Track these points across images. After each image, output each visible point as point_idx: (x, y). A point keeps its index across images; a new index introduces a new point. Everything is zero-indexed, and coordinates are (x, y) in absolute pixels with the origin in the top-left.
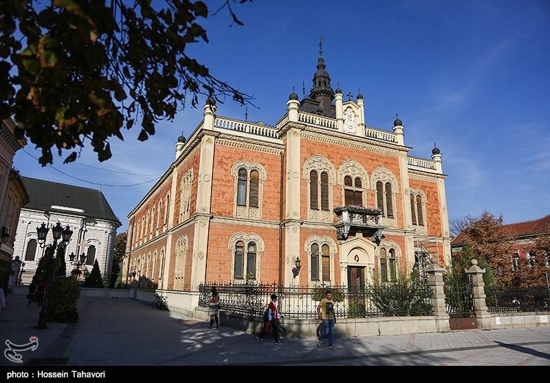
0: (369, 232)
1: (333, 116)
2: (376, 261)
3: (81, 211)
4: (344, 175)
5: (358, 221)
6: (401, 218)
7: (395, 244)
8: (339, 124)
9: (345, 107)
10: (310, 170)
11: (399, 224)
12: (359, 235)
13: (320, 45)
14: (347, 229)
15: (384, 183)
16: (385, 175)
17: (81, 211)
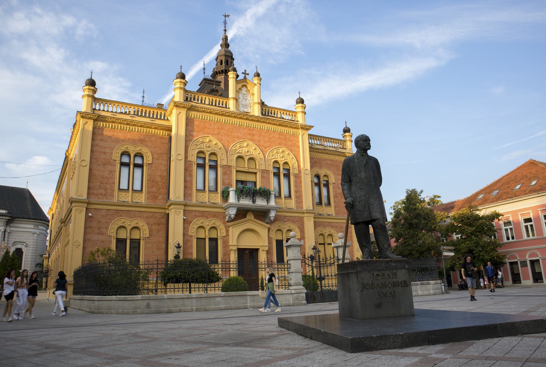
0: (262, 215)
1: (225, 94)
2: (270, 242)
3: (4, 212)
4: (236, 156)
5: (246, 202)
6: (299, 198)
7: (293, 226)
8: (231, 104)
9: (240, 86)
10: (197, 151)
11: (297, 202)
12: (250, 216)
13: (225, 23)
15: (281, 163)
16: (282, 155)
17: (4, 212)
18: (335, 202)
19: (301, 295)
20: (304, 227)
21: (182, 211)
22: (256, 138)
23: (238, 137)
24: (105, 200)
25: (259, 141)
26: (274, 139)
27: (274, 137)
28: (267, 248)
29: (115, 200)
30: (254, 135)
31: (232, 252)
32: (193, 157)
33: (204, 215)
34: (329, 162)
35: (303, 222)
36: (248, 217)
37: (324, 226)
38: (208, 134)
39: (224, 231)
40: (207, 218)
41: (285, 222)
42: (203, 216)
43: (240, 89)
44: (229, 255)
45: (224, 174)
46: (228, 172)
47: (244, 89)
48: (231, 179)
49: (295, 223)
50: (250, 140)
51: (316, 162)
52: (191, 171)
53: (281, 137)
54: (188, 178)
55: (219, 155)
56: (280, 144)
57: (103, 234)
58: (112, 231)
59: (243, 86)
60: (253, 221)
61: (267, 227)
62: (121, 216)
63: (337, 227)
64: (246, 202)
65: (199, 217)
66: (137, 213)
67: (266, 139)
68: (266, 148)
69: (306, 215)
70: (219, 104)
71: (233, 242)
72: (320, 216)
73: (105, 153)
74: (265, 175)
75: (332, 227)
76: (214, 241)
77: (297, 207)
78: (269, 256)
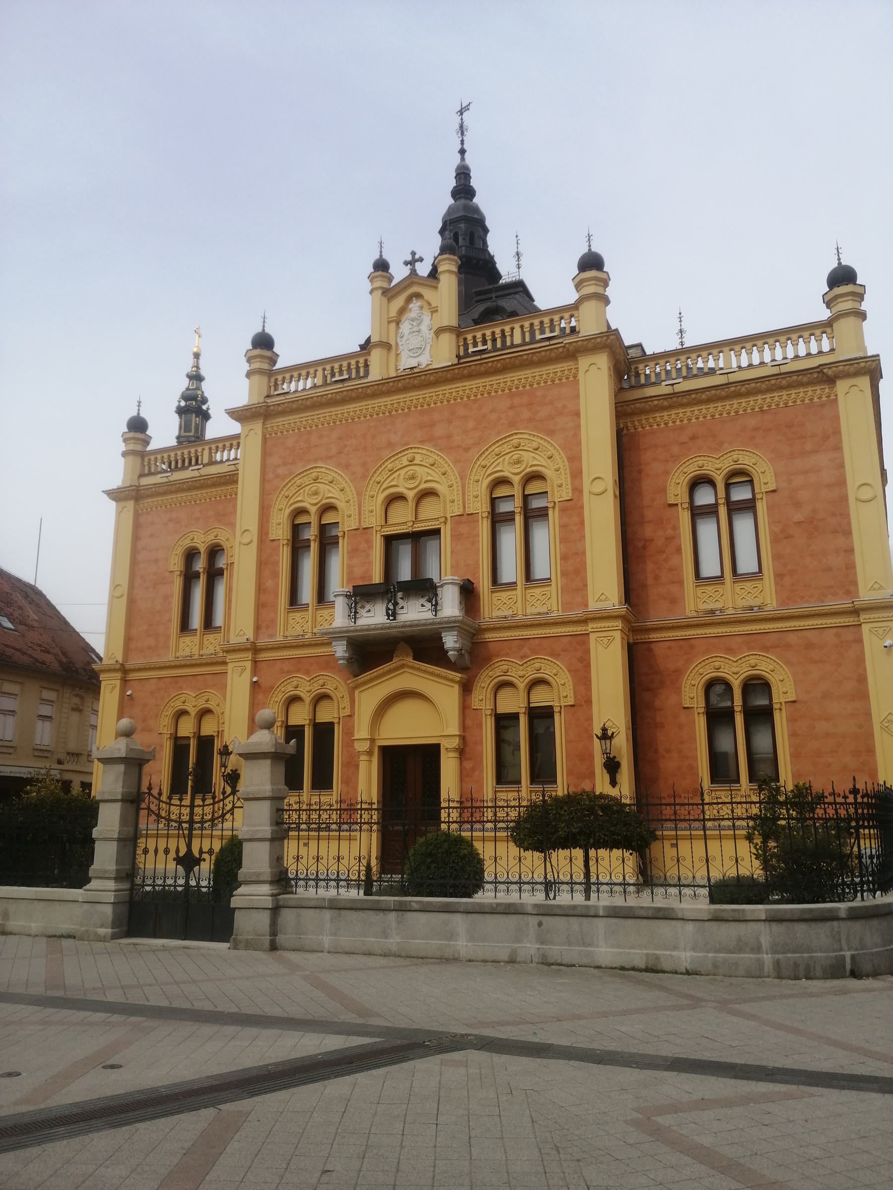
0: (425, 647)
4: (381, 497)
7: (549, 668)
10: (288, 511)
13: (462, 129)
14: (340, 650)
18: (776, 557)
19: (99, 907)
20: (588, 666)
21: (248, 665)
22: (439, 430)
23: (390, 445)
24: (155, 660)
25: (449, 437)
26: (493, 417)
27: (493, 411)
28: (455, 742)
29: (169, 657)
30: (432, 425)
31: (363, 758)
32: (280, 531)
33: (299, 665)
34: (752, 422)
35: (588, 652)
36: (396, 662)
37: (730, 650)
38: (316, 460)
39: (346, 703)
40: (307, 673)
41: (523, 657)
42: (298, 671)
43: (402, 311)
44: (357, 766)
45: (353, 552)
46: (363, 546)
47: (415, 305)
48: (370, 563)
49: (556, 655)
50: (422, 442)
51: (693, 438)
52: (276, 564)
53: (517, 401)
54: (269, 583)
55: (340, 505)
56: (512, 424)
57: (150, 730)
58: (164, 725)
59: (409, 300)
60: (412, 668)
61: (452, 681)
62: (181, 688)
63: (788, 646)
64: (374, 617)
65: (289, 672)
66: (207, 677)
67: (471, 424)
68: (467, 450)
69: (591, 626)
70: (333, 375)
71: (362, 731)
72: (708, 619)
73: (156, 561)
74: (464, 529)
75: (766, 649)
76: (324, 733)
77: (567, 606)
78: (468, 765)
